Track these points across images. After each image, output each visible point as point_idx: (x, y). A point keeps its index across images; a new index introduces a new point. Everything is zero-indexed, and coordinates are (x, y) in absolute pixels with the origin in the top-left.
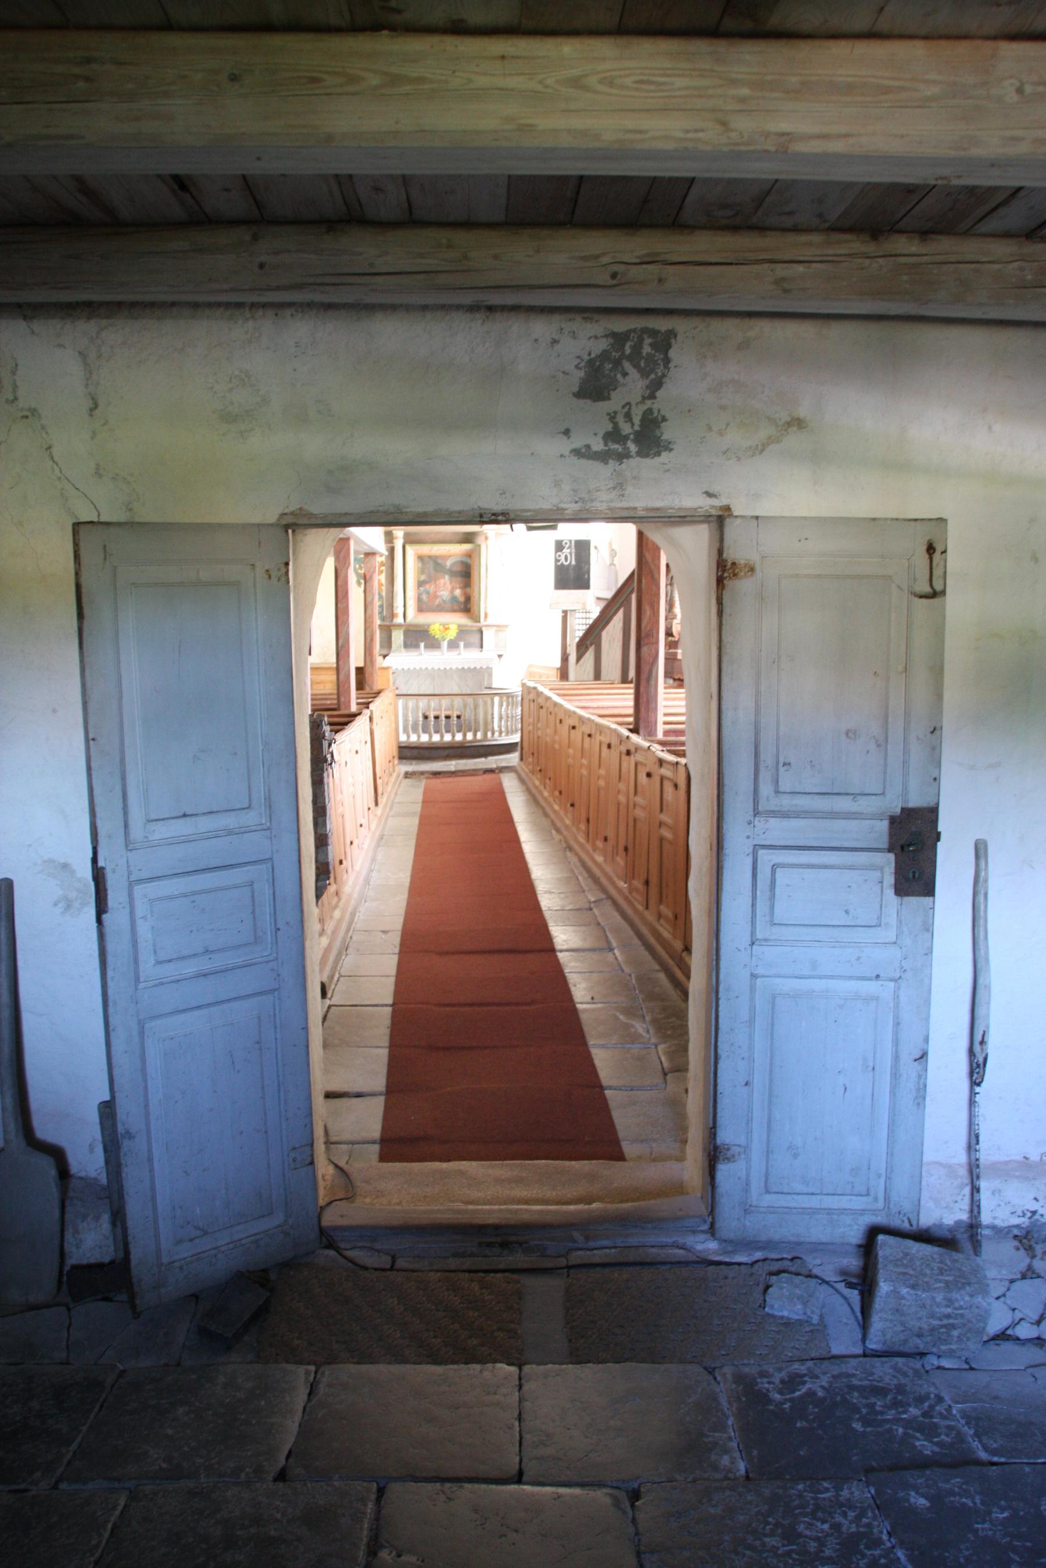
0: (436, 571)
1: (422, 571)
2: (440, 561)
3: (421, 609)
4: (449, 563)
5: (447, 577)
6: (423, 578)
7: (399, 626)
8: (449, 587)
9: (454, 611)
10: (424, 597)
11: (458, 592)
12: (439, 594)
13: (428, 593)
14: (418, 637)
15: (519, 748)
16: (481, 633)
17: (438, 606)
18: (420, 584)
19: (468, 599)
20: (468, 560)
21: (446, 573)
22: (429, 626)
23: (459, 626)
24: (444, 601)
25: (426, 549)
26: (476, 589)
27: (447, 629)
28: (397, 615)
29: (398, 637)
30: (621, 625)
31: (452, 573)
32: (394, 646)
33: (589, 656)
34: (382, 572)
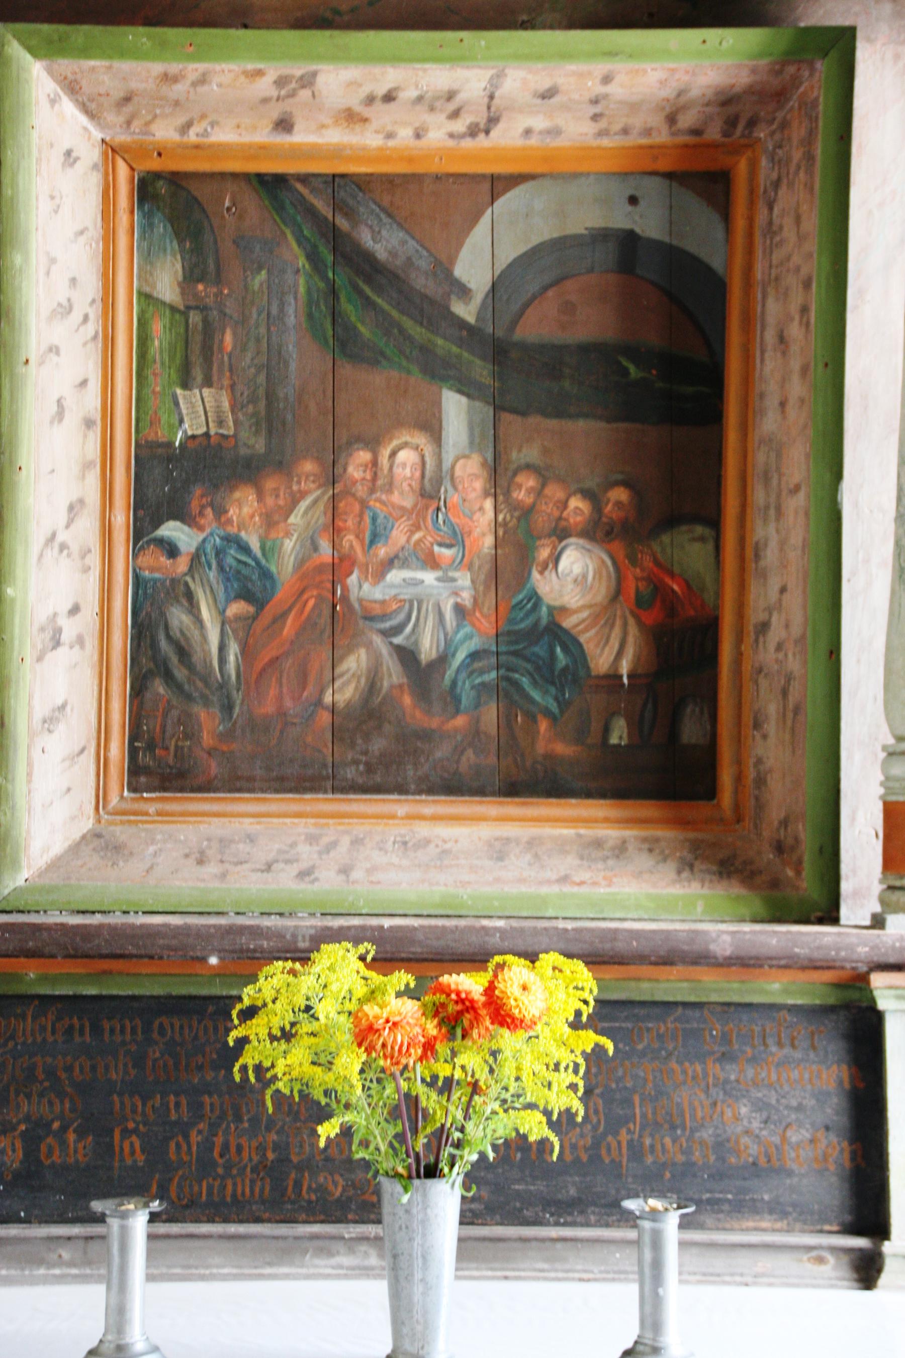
0: (344, 344)
1: (183, 342)
2: (382, 241)
3: (166, 749)
4: (476, 264)
5: (455, 409)
6: (197, 413)
8: (482, 519)
9: (526, 781)
10: (209, 626)
11: (573, 577)
12: (361, 588)
13: (250, 584)
17: (370, 713)
18: (164, 482)
19: (686, 648)
20: (703, 238)
21: (440, 371)
22: (252, 952)
24: (419, 672)
26: (781, 540)
27: (456, 1019)
31: (516, 374)
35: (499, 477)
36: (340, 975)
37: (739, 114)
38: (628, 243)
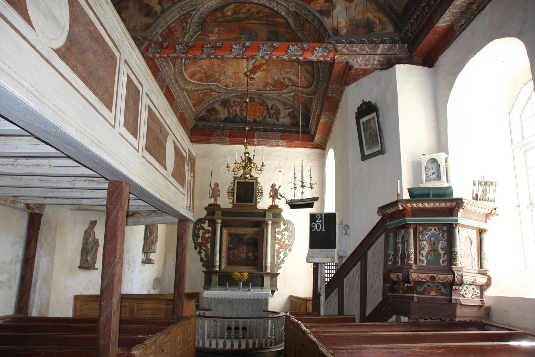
3: (229, 263)
4: (246, 238)
5: (244, 246)
6: (231, 246)
7: (217, 272)
8: (246, 252)
10: (232, 256)
11: (250, 254)
13: (234, 254)
14: (227, 280)
15: (283, 353)
16: (263, 277)
18: (229, 249)
19: (256, 258)
23: (249, 273)
24: (242, 259)
25: (233, 230)
27: (242, 275)
28: (215, 266)
29: (215, 279)
30: (359, 273)
31: (248, 244)
32: (212, 284)
33: (334, 296)
34: (209, 242)
35: (246, 249)
36: (237, 273)
37: (259, 231)
38: (253, 237)
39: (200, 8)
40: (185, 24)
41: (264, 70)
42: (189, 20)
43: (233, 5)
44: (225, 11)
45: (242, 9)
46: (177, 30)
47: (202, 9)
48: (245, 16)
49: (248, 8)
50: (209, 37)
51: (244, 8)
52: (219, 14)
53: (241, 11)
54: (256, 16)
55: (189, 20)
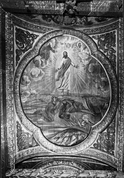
39: (88, 147)
40: (99, 141)
41: (57, 71)
42: (96, 142)
43: (72, 143)
44: (76, 140)
45: (67, 141)
46: (104, 142)
47: (88, 146)
48: (66, 134)
49: (64, 142)
50: (88, 119)
51: (65, 141)
52: (80, 138)
53: (67, 138)
54: (59, 135)
55: (96, 142)
